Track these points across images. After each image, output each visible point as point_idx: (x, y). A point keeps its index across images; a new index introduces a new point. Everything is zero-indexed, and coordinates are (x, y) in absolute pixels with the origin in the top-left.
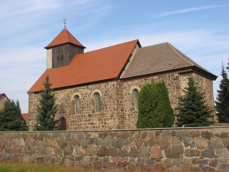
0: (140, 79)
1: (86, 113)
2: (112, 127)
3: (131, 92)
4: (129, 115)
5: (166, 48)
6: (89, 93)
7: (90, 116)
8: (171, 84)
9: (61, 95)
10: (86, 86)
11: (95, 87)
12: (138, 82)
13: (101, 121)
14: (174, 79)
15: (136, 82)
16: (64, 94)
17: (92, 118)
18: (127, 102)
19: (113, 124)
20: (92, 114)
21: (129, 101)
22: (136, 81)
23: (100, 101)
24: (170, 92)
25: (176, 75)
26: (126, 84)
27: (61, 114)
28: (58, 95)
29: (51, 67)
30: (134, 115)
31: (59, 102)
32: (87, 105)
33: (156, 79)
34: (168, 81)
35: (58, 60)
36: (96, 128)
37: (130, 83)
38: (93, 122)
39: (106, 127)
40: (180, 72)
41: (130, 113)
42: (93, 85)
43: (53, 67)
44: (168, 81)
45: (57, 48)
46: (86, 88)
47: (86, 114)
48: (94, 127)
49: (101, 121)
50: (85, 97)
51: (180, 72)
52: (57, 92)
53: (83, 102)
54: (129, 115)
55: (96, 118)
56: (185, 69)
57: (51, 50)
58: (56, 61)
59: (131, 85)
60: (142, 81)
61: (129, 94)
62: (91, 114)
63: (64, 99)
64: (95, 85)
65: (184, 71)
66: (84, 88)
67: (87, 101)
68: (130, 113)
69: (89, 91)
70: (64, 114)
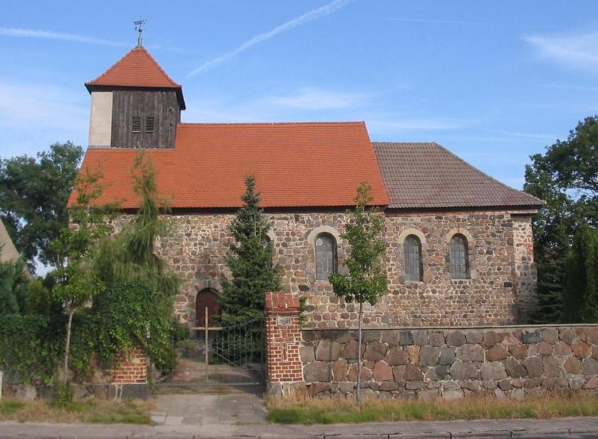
0: (423, 214)
1: (293, 280)
2: (370, 318)
3: (401, 240)
4: (396, 293)
5: (434, 155)
6: (304, 232)
7: (303, 288)
8: (498, 234)
9: (204, 227)
10: (293, 215)
11: (320, 220)
12: (419, 221)
13: (339, 303)
14: (503, 225)
15: (415, 221)
16: (216, 227)
17: (310, 293)
18: (391, 262)
19: (375, 311)
20: (312, 284)
21: (394, 260)
22: (416, 218)
23: (337, 253)
24: (495, 249)
25: (507, 215)
26: (389, 222)
27: (206, 278)
28: (193, 228)
29: (107, 143)
30: (407, 293)
31: (195, 245)
32: (297, 261)
33: (464, 220)
34: (490, 227)
35: (134, 128)
36: (323, 320)
37: (399, 219)
38: (313, 305)
39: (353, 317)
40: (516, 212)
41: (398, 287)
42: (316, 214)
43: (113, 145)
44: (490, 227)
45: (132, 97)
46: (291, 218)
47: (291, 284)
48: (318, 318)
49: (339, 303)
50: (289, 240)
51: (516, 212)
52: (190, 217)
53: (281, 252)
54: (396, 293)
55: (324, 294)
56: (515, 209)
57: (106, 98)
58: (128, 128)
59: (401, 224)
60: (429, 220)
61: (394, 245)
62: (308, 284)
63: (215, 240)
64: (322, 214)
65: (521, 212)
66: (286, 219)
67: (297, 251)
68: (398, 287)
69: (304, 228)
70: (215, 279)
